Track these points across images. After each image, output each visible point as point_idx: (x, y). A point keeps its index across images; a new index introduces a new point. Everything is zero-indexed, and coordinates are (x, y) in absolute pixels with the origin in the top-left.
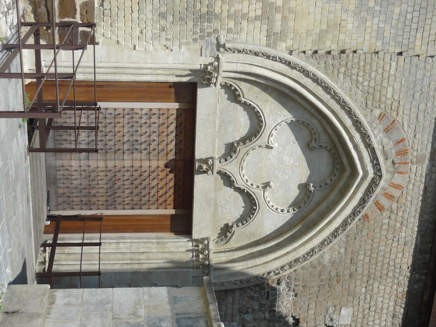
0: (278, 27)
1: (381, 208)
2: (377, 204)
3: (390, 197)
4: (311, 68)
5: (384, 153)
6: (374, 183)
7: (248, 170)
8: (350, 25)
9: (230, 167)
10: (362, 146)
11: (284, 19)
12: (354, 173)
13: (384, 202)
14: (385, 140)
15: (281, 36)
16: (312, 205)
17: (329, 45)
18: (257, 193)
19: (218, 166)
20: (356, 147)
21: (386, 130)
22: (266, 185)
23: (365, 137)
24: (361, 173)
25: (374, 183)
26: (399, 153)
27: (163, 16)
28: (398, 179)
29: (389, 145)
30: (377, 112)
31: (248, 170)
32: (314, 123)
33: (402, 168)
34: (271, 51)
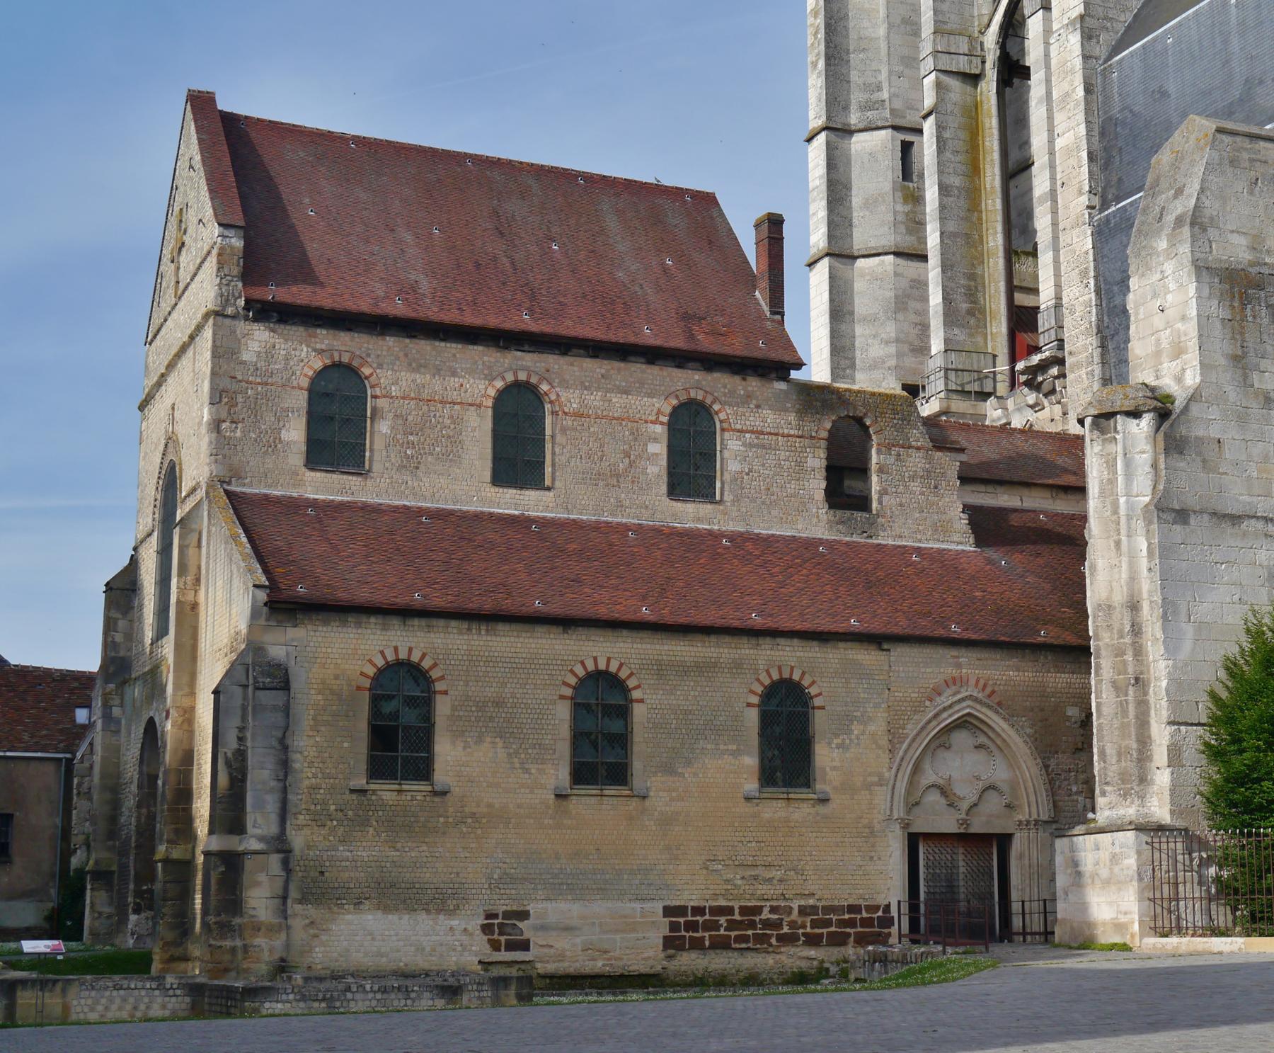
0: (875, 779)
1: (993, 692)
2: (989, 696)
3: (985, 686)
4: (901, 753)
5: (954, 694)
6: (976, 700)
7: (966, 792)
8: (871, 728)
9: (965, 806)
10: (951, 711)
11: (870, 775)
12: (969, 714)
13: (988, 690)
14: (946, 694)
15: (880, 775)
16: (989, 743)
17: (884, 742)
18: (981, 785)
19: (963, 816)
20: (950, 716)
21: (940, 694)
22: (978, 779)
23: (945, 709)
24: (967, 711)
25: (976, 700)
26: (955, 683)
27: (872, 858)
28: (972, 682)
29: (949, 692)
30: (927, 703)
31: (966, 792)
32: (933, 746)
33: (965, 679)
34: (891, 782)
